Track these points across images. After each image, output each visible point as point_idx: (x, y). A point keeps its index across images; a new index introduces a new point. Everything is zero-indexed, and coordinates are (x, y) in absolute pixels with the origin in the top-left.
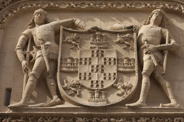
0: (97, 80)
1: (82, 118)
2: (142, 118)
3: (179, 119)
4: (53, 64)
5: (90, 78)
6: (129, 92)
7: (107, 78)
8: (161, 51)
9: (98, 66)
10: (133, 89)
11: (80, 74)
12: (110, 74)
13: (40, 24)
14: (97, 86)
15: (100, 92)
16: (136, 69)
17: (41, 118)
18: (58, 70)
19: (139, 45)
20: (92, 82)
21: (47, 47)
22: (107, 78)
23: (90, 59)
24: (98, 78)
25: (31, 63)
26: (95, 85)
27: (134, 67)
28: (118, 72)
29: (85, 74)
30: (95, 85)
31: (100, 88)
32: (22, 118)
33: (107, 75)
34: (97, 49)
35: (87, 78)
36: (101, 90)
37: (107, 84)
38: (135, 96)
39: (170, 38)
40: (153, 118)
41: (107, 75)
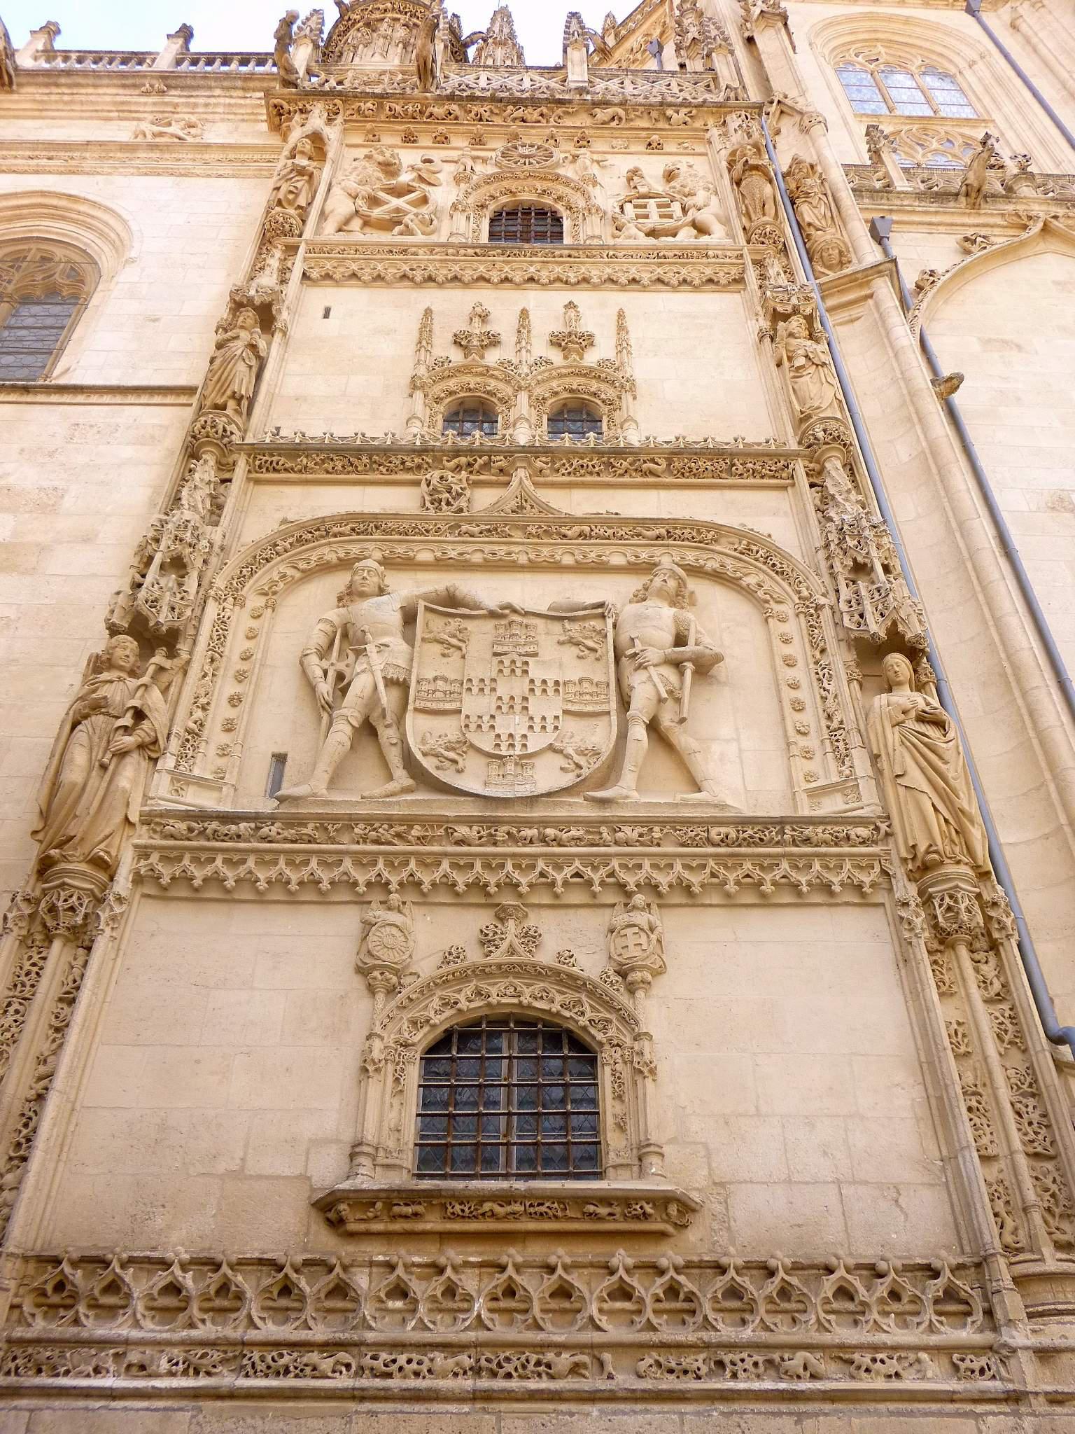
1: (471, 827)
2: (627, 829)
3: (723, 830)
12: (544, 718)
16: (613, 705)
17: (362, 826)
18: (410, 707)
26: (504, 746)
31: (518, 751)
32: (311, 825)
33: (537, 720)
35: (485, 727)
36: (521, 757)
40: (657, 829)
41: (537, 720)
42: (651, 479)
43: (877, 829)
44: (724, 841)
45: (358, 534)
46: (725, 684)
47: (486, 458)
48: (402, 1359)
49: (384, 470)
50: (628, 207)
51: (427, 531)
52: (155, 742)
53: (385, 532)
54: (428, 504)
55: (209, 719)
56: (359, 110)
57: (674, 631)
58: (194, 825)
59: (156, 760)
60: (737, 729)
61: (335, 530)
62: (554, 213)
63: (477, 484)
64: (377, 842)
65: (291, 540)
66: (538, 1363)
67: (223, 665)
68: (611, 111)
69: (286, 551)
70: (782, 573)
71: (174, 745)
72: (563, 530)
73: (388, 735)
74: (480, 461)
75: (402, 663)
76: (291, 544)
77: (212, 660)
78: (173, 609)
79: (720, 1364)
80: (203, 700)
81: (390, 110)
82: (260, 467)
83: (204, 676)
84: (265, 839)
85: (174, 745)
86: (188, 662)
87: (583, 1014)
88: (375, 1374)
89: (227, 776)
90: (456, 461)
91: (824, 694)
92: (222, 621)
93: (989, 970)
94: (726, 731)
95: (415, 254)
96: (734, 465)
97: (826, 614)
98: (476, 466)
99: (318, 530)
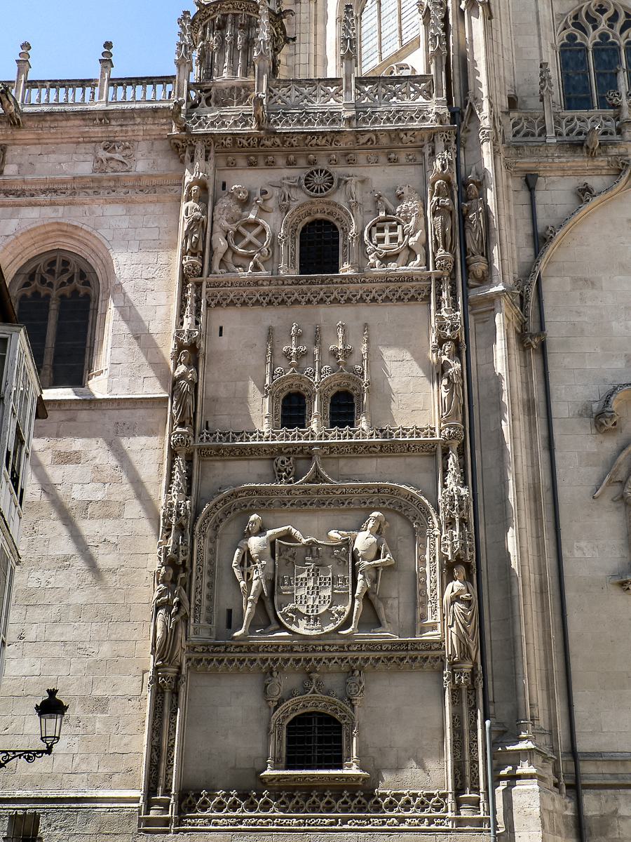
4: (270, 584)
5: (306, 602)
6: (343, 618)
7: (322, 602)
8: (376, 568)
9: (313, 588)
10: (346, 613)
15: (316, 620)
19: (354, 559)
22: (322, 602)
25: (250, 583)
26: (310, 610)
28: (332, 593)
30: (310, 610)
31: (315, 614)
34: (312, 566)
37: (322, 610)
38: (347, 624)
40: (364, 646)
43: (441, 644)
44: (387, 650)
46: (396, 570)
47: (301, 448)
48: (285, 821)
50: (374, 229)
53: (260, 494)
54: (277, 477)
56: (223, 143)
57: (376, 550)
60: (399, 592)
62: (335, 228)
64: (267, 652)
66: (321, 821)
68: (367, 136)
71: (192, 611)
73: (268, 605)
74: (298, 449)
75: (271, 572)
78: (182, 551)
79: (370, 822)
80: (199, 590)
81: (240, 143)
83: (198, 577)
84: (230, 652)
85: (192, 611)
86: (192, 573)
87: (337, 713)
88: (278, 825)
92: (200, 550)
93: (471, 697)
94: (394, 594)
95: (262, 285)
97: (437, 539)
99: (232, 495)
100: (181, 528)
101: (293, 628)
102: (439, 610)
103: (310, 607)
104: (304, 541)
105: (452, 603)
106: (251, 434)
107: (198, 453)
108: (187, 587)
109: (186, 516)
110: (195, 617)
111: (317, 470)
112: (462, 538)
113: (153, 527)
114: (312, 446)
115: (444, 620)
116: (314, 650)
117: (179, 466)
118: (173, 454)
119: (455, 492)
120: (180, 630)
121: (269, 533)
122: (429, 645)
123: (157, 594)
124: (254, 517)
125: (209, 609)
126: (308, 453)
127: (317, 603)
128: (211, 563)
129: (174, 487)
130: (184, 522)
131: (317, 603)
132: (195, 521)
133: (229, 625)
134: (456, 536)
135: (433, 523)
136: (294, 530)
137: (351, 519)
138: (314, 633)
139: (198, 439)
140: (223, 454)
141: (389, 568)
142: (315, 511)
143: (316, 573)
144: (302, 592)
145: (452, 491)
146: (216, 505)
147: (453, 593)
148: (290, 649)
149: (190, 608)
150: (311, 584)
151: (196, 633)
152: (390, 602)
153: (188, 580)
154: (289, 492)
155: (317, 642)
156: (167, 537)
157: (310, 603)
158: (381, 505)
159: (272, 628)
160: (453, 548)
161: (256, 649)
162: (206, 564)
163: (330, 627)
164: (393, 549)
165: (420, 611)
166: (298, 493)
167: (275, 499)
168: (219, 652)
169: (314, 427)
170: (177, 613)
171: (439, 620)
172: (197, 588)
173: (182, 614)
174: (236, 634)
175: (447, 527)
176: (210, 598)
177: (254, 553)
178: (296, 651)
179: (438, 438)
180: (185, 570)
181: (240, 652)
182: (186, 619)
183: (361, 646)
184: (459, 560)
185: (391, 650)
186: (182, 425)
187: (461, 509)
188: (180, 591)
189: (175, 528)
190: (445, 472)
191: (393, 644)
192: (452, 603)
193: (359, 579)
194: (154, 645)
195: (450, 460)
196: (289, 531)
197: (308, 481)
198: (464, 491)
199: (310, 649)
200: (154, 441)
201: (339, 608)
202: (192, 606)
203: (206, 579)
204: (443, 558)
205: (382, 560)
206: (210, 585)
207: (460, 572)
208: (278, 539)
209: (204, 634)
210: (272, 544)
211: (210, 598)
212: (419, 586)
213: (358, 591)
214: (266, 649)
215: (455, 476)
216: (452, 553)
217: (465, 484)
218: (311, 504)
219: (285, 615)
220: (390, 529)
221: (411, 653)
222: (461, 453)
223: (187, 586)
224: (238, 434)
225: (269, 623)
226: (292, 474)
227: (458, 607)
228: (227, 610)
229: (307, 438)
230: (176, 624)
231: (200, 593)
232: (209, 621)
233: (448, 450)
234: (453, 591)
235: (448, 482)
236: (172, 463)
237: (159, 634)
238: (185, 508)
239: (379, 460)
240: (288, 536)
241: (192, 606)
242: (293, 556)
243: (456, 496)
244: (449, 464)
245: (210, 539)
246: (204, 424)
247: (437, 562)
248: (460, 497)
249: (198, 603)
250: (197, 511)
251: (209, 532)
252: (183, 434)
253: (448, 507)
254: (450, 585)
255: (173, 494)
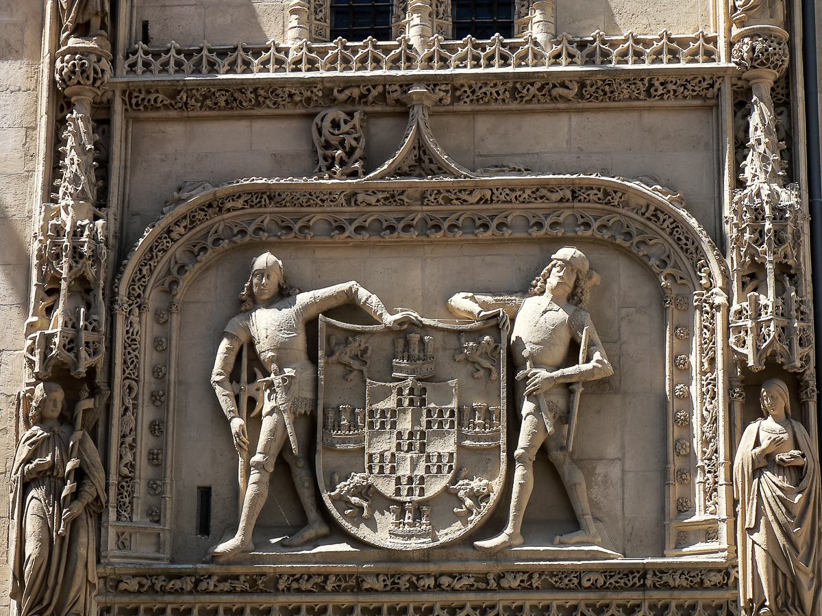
0: (408, 473)
3: (593, 577)
4: (303, 424)
5: (393, 470)
6: (486, 507)
7: (434, 470)
8: (567, 387)
9: (411, 434)
10: (493, 497)
11: (371, 456)
13: (269, 304)
14: (410, 492)
15: (418, 514)
19: (514, 364)
20: (398, 480)
21: (288, 383)
23: (394, 413)
24: (413, 469)
25: (254, 422)
27: (495, 438)
28: (460, 446)
29: (382, 455)
31: (416, 498)
34: (409, 382)
37: (434, 488)
38: (494, 524)
39: (591, 344)
40: (536, 576)
42: (562, 105)
43: (728, 574)
44: (593, 588)
45: (252, 206)
46: (616, 392)
47: (380, 88)
49: (271, 105)
51: (323, 201)
52: (98, 498)
53: (279, 204)
54: (322, 163)
55: (138, 459)
58: (144, 581)
59: (100, 516)
60: (623, 447)
61: (229, 205)
63: (369, 116)
64: (299, 591)
65: (184, 224)
67: (141, 391)
69: (182, 235)
70: (687, 250)
71: (113, 492)
72: (464, 196)
73: (301, 475)
74: (374, 93)
75: (308, 395)
76: (185, 227)
77: (130, 388)
78: (87, 343)
80: (129, 440)
82: (137, 104)
83: (126, 409)
84: (207, 592)
85: (113, 492)
86: (111, 398)
89: (162, 520)
90: (347, 92)
91: (705, 413)
92: (131, 341)
94: (612, 451)
96: (651, 85)
97: (719, 316)
98: (370, 98)
100: (83, 287)
101: (363, 532)
102: (722, 490)
103: (404, 481)
104: (389, 319)
105: (757, 472)
106: (257, 54)
107: (124, 101)
108: (99, 433)
109: (95, 257)
110: (120, 506)
111: (420, 146)
112: (783, 312)
113: (14, 284)
114: (407, 83)
115: (736, 515)
116: (414, 588)
117: (77, 135)
118: (61, 103)
119: (765, 198)
120: (83, 539)
121: (303, 298)
122: (697, 576)
123: (24, 451)
124: (264, 260)
125: (154, 487)
126: (397, 101)
127: (420, 471)
128: (159, 373)
129: (64, 186)
130: (91, 273)
131: (420, 471)
132: (118, 269)
133: (204, 527)
134: (766, 307)
135: (710, 275)
136: (363, 293)
137: (505, 264)
138: (414, 544)
139: (123, 66)
140: (186, 104)
141: (598, 386)
142: (411, 245)
143: (418, 399)
144: (384, 445)
145: (758, 195)
146: (169, 231)
147: (758, 450)
148: (356, 584)
149: (107, 485)
150: (405, 424)
151: (122, 545)
152: (600, 469)
153: (102, 418)
154: (351, 198)
155: (419, 568)
156: (49, 310)
157: (404, 471)
158: (581, 231)
159: (309, 533)
160: (759, 338)
161: (272, 584)
162: (146, 375)
163: (454, 531)
164: (609, 339)
165: (675, 491)
166: (373, 200)
167: (317, 216)
168: (181, 591)
169: (413, 35)
170: (75, 496)
171: (722, 512)
172: (124, 436)
173: (87, 498)
174: (221, 548)
175: (744, 284)
176: (155, 458)
177: (265, 348)
178: (370, 591)
179: (723, 63)
180: (94, 392)
181: (232, 592)
182: (97, 511)
183: (530, 577)
184: (773, 368)
185: (604, 588)
186: (82, 30)
187: (780, 241)
188: (81, 442)
189: (69, 289)
190: (741, 147)
191: (609, 572)
192: (757, 472)
193: (524, 413)
194: (19, 575)
195: (754, 119)
196: (351, 296)
197: (398, 172)
198: (787, 197)
199: (403, 583)
200: (11, 71)
201: (476, 484)
202: (113, 479)
203: (147, 414)
204: (735, 361)
205: (583, 367)
206: (157, 428)
207: (776, 395)
208: (326, 314)
209: (143, 548)
210: (311, 326)
211: (155, 458)
212: (674, 432)
213: (523, 441)
214: (295, 585)
215: (764, 158)
216: (757, 349)
217: (789, 179)
218: (407, 228)
219: (342, 502)
220: (600, 291)
221: (656, 595)
222: (782, 102)
223: (101, 430)
224: (222, 54)
225: (304, 522)
226: (358, 153)
227: (771, 482)
228: (198, 488)
229: (395, 63)
230: (73, 524)
231: (132, 447)
232: (155, 515)
233: (748, 92)
234: (757, 443)
235: (748, 173)
236: (58, 125)
237: (31, 548)
238: (93, 237)
239: (576, 119)
240: (349, 308)
241: (113, 479)
242: (361, 356)
243: (767, 208)
244: (752, 129)
245: (157, 314)
246: (137, 28)
247: (720, 374)
248: (779, 212)
249: (125, 471)
250: (123, 247)
251: (153, 298)
252: (85, 52)
253: (747, 236)
254: (752, 428)
255: (63, 203)
